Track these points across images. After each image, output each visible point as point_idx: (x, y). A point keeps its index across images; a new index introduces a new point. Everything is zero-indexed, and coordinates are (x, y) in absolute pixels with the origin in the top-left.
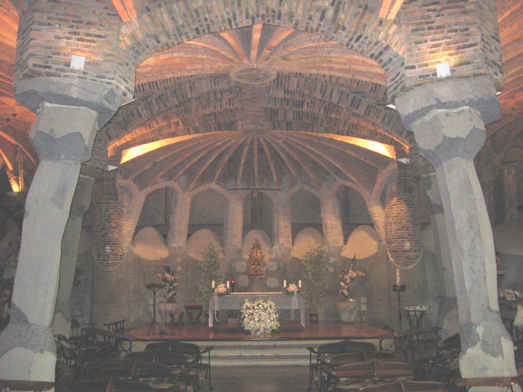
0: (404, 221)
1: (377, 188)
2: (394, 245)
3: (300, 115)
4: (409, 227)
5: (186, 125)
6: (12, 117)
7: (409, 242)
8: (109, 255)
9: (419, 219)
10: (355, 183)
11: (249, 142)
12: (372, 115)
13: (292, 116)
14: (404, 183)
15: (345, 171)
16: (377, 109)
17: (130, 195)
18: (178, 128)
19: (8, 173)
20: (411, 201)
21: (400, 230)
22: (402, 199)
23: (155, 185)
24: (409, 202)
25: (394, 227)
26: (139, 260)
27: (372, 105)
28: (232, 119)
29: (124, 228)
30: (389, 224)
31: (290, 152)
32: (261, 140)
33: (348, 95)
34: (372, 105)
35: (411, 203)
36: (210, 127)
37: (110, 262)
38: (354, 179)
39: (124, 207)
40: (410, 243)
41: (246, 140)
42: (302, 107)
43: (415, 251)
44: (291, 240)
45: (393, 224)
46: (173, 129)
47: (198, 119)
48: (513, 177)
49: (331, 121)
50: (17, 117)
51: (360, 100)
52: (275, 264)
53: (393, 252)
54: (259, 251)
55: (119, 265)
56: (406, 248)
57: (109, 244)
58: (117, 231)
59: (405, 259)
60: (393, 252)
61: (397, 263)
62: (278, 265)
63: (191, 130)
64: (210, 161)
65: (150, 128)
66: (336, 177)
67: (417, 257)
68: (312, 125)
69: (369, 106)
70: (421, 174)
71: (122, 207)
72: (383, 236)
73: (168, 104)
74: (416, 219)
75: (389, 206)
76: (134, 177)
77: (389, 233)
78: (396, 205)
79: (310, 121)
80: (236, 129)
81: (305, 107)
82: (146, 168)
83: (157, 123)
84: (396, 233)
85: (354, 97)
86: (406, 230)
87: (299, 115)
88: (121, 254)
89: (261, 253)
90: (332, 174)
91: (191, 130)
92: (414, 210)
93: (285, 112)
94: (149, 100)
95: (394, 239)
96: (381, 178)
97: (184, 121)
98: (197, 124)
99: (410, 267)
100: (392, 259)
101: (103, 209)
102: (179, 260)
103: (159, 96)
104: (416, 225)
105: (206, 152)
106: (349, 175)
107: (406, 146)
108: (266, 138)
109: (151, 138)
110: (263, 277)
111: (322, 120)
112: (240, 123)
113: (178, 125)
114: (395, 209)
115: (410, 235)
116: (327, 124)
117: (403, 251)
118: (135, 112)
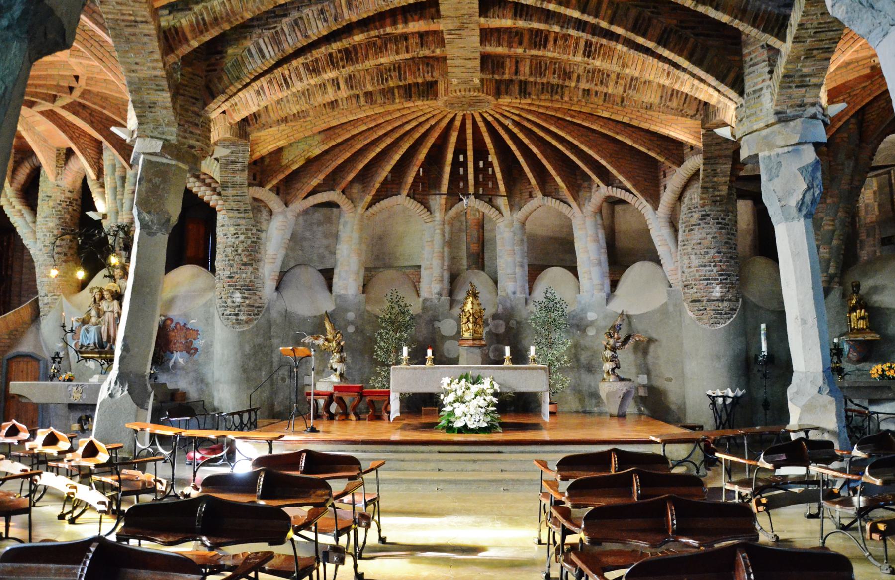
0: (712, 252)
1: (667, 198)
2: (695, 290)
3: (541, 67)
4: (721, 261)
5: (352, 87)
6: (73, 84)
8: (238, 306)
10: (631, 192)
11: (458, 123)
12: (672, 45)
13: (527, 68)
14: (714, 188)
15: (614, 172)
16: (680, 36)
17: (271, 212)
18: (339, 92)
19: (90, 183)
21: (705, 266)
22: (708, 215)
23: (310, 198)
24: (720, 221)
25: (695, 261)
26: (287, 315)
27: (671, 30)
28: (429, 78)
29: (261, 264)
30: (686, 257)
31: (526, 141)
32: (479, 119)
33: (629, 9)
34: (671, 30)
36: (393, 94)
37: (240, 318)
38: (629, 185)
39: (262, 231)
40: (721, 287)
41: (453, 120)
42: (545, 47)
43: (730, 300)
44: (527, 285)
45: (693, 257)
46: (331, 95)
47: (373, 79)
48: (874, 192)
49: (593, 78)
50: (82, 82)
51: (650, 19)
52: (501, 322)
53: (692, 302)
54: (475, 302)
55: (255, 322)
57: (237, 289)
58: (251, 269)
59: (712, 313)
60: (692, 302)
61: (699, 320)
62: (507, 323)
63: (362, 100)
64: (397, 157)
65: (288, 87)
66: (601, 184)
67: (732, 310)
68: (562, 88)
69: (666, 28)
70: (761, 151)
71: (258, 231)
72: (676, 280)
73: (310, 33)
75: (686, 227)
76: (275, 182)
77: (686, 270)
78: (699, 225)
79: (559, 77)
80: (435, 96)
81: (551, 45)
82: (295, 167)
83: (301, 80)
84: (697, 271)
85: (640, 14)
86: (714, 266)
87: (539, 66)
88: (257, 305)
89: (479, 305)
90: (594, 177)
91: (362, 100)
92: (728, 234)
93: (517, 62)
94: (279, 29)
95: (695, 280)
96: (674, 179)
97: (350, 80)
98: (370, 88)
100: (691, 314)
101: (230, 236)
102: (351, 316)
103: (296, 21)
104: (731, 257)
105: (389, 141)
106: (621, 178)
107: (730, 103)
108: (485, 115)
109: (296, 112)
110: (483, 342)
111: (579, 77)
112: (441, 87)
113: (339, 88)
114: (696, 232)
115: (722, 275)
116: (587, 82)
117: (709, 300)
118: (253, 51)
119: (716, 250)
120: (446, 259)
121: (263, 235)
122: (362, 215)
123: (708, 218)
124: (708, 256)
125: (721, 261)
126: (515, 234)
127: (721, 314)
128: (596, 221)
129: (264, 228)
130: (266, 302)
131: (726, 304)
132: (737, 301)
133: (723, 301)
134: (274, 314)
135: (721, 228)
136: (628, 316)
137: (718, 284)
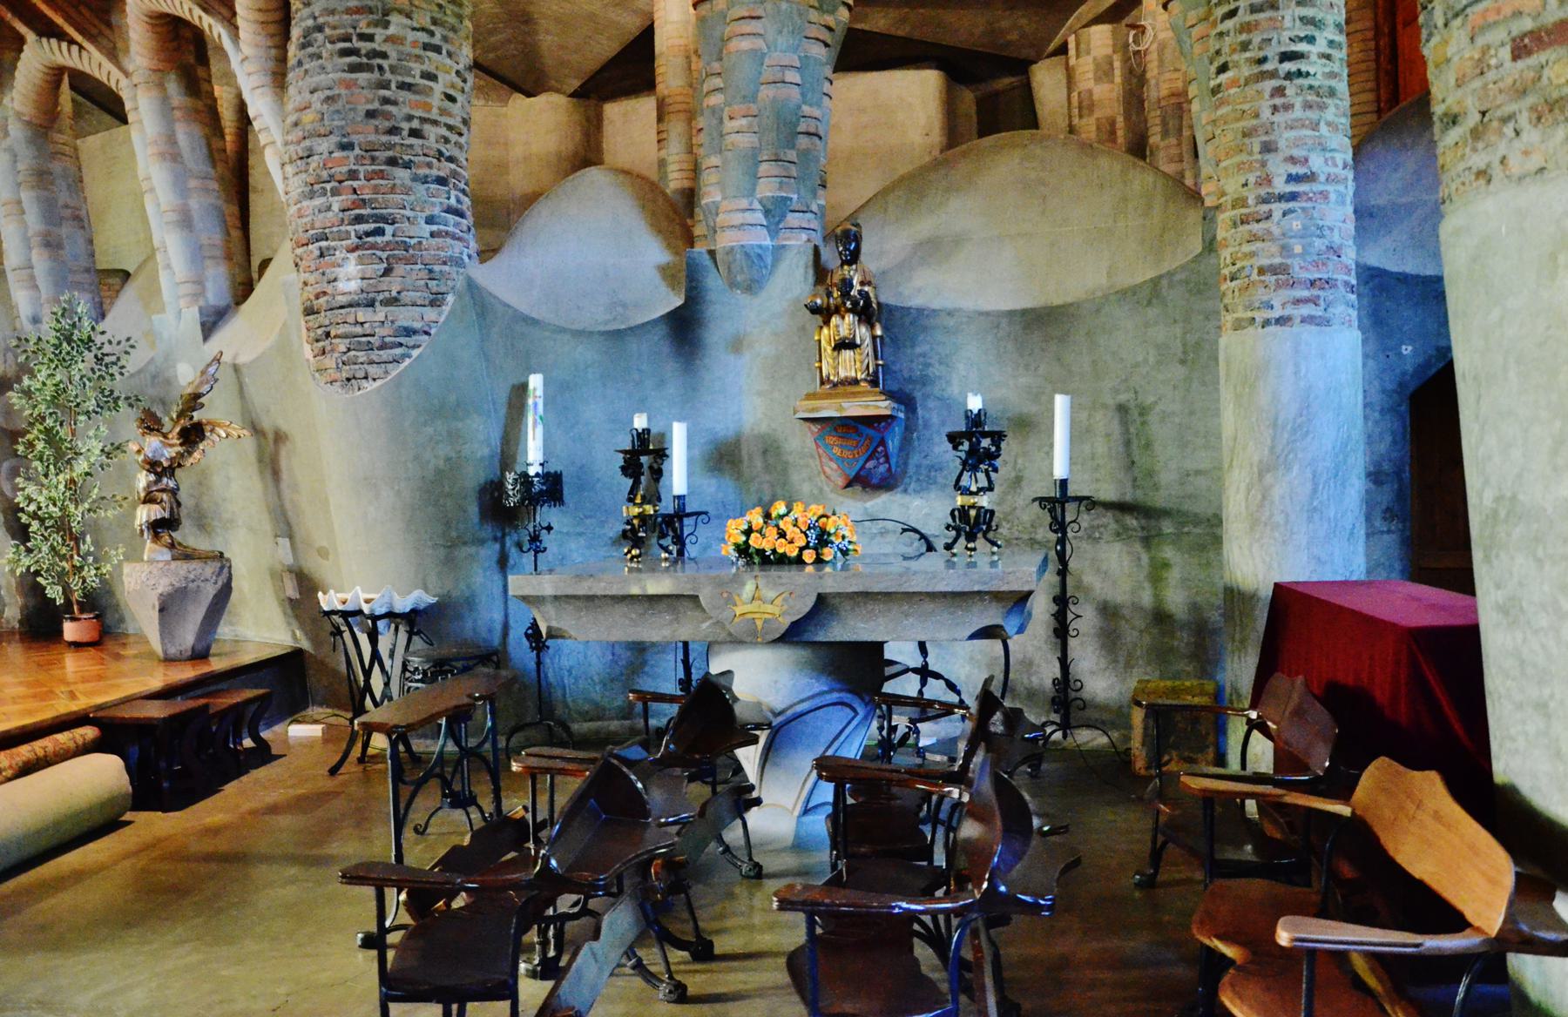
0: (323, 146)
4: (353, 175)
7: (353, 257)
9: (414, 133)
20: (370, 38)
21: (311, 195)
22: (320, 29)
24: (356, 44)
35: (365, 46)
40: (360, 261)
56: (342, 286)
67: (409, 332)
74: (394, 131)
86: (335, 192)
99: (369, 386)
104: (392, 162)
115: (359, 219)
119: (334, 139)
123: (320, 37)
124: (314, 162)
125: (353, 175)
126: (15, 158)
127: (370, 347)
128: (165, 98)
131: (381, 313)
132: (436, 301)
133: (371, 304)
135: (353, 68)
136: (236, 368)
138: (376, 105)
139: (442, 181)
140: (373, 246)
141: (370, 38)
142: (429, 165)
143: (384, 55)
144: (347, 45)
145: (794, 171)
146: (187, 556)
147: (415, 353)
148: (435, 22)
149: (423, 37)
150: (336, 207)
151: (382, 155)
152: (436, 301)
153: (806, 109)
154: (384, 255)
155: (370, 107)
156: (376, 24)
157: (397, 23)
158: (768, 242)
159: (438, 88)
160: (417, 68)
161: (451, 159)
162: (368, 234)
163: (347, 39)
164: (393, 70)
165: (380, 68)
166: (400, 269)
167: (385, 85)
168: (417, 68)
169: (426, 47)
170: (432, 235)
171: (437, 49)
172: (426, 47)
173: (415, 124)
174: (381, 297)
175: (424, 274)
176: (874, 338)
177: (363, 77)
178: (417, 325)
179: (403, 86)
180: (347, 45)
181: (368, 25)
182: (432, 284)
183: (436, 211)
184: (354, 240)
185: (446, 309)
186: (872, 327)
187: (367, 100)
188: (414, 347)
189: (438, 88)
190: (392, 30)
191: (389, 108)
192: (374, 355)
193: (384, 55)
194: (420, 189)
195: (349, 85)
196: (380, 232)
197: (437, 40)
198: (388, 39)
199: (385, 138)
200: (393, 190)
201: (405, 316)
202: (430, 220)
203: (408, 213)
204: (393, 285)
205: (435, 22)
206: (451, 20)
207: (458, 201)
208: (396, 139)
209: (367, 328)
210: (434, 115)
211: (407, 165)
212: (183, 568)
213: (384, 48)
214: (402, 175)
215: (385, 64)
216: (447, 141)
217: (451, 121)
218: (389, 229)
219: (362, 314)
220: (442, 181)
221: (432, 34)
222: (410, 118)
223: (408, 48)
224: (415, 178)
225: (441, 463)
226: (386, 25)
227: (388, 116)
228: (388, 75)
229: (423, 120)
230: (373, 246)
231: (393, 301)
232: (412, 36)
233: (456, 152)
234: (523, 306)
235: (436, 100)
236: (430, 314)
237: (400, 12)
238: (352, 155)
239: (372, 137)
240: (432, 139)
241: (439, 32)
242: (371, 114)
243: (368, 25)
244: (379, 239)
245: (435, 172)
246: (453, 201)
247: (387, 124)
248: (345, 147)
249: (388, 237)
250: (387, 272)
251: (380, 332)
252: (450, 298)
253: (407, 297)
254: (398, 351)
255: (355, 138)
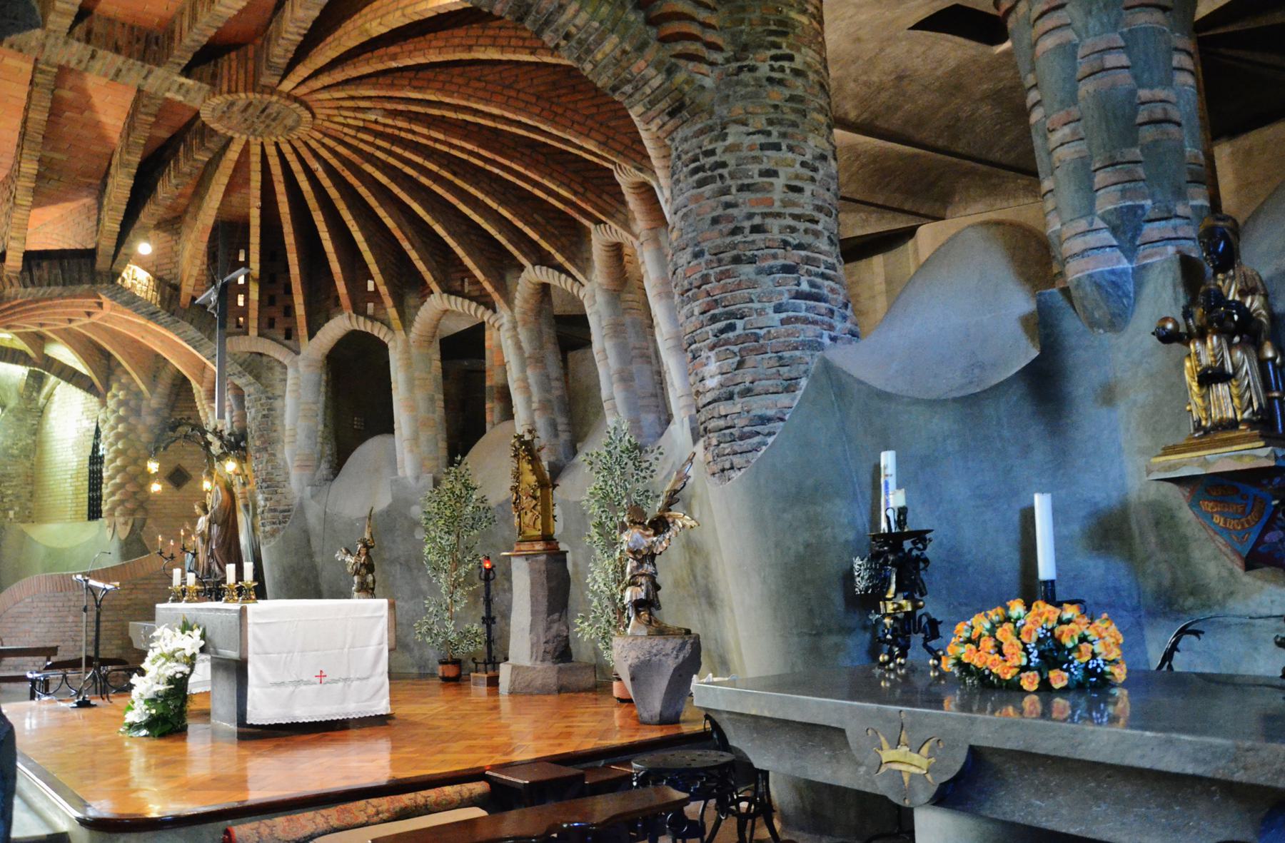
4: (705, 279)
7: (712, 354)
9: (756, 229)
20: (711, 153)
39: (274, 398)
58: (266, 456)
67: (764, 420)
88: (282, 508)
99: (736, 475)
104: (737, 260)
115: (714, 319)
119: (689, 250)
120: (534, 389)
121: (277, 404)
122: (407, 342)
125: (705, 279)
129: (278, 392)
130: (297, 501)
131: (737, 406)
133: (730, 397)
134: (313, 517)
135: (701, 184)
137: (712, 348)
138: (720, 211)
139: (788, 269)
140: (727, 342)
141: (711, 153)
142: (775, 257)
143: (723, 165)
144: (697, 164)
145: (1140, 171)
146: (662, 631)
147: (770, 440)
148: (771, 122)
149: (760, 139)
150: (696, 313)
151: (727, 256)
152: (789, 388)
153: (1144, 94)
154: (736, 349)
155: (715, 214)
156: (716, 139)
157: (734, 134)
158: (1125, 264)
159: (779, 183)
160: (755, 169)
161: (800, 247)
162: (722, 331)
163: (695, 159)
164: (732, 176)
165: (721, 176)
166: (751, 360)
167: (726, 191)
168: (755, 169)
169: (763, 147)
170: (783, 322)
171: (777, 147)
172: (763, 147)
173: (757, 220)
174: (737, 389)
175: (773, 362)
176: (1262, 363)
177: (708, 189)
178: (770, 413)
179: (742, 188)
180: (697, 164)
181: (711, 142)
182: (783, 370)
183: (785, 298)
184: (712, 340)
185: (799, 393)
186: (1259, 349)
187: (710, 208)
188: (769, 434)
189: (779, 183)
190: (730, 140)
191: (730, 211)
192: (738, 446)
193: (723, 165)
194: (767, 282)
195: (697, 199)
196: (731, 328)
197: (774, 139)
198: (727, 150)
199: (728, 240)
200: (739, 287)
201: (760, 406)
202: (778, 309)
203: (756, 305)
204: (746, 376)
205: (771, 122)
206: (792, 117)
207: (812, 285)
208: (739, 238)
209: (729, 422)
210: (777, 207)
211: (752, 261)
212: (658, 641)
213: (725, 158)
214: (747, 270)
215: (725, 172)
216: (793, 230)
217: (797, 211)
218: (740, 324)
219: (723, 408)
220: (788, 269)
221: (769, 134)
222: (750, 216)
223: (745, 153)
224: (760, 272)
225: (801, 549)
226: (724, 137)
227: (731, 219)
228: (729, 182)
229: (764, 215)
230: (727, 342)
231: (747, 392)
232: (747, 141)
233: (808, 239)
234: (878, 383)
235: (778, 194)
236: (784, 400)
237: (736, 122)
238: (702, 260)
239: (719, 241)
240: (776, 230)
241: (775, 131)
242: (715, 221)
243: (711, 142)
244: (731, 335)
245: (781, 262)
246: (805, 287)
247: (731, 226)
248: (696, 255)
249: (739, 331)
250: (740, 365)
251: (740, 422)
252: (804, 382)
253: (759, 386)
254: (756, 439)
255: (706, 246)
